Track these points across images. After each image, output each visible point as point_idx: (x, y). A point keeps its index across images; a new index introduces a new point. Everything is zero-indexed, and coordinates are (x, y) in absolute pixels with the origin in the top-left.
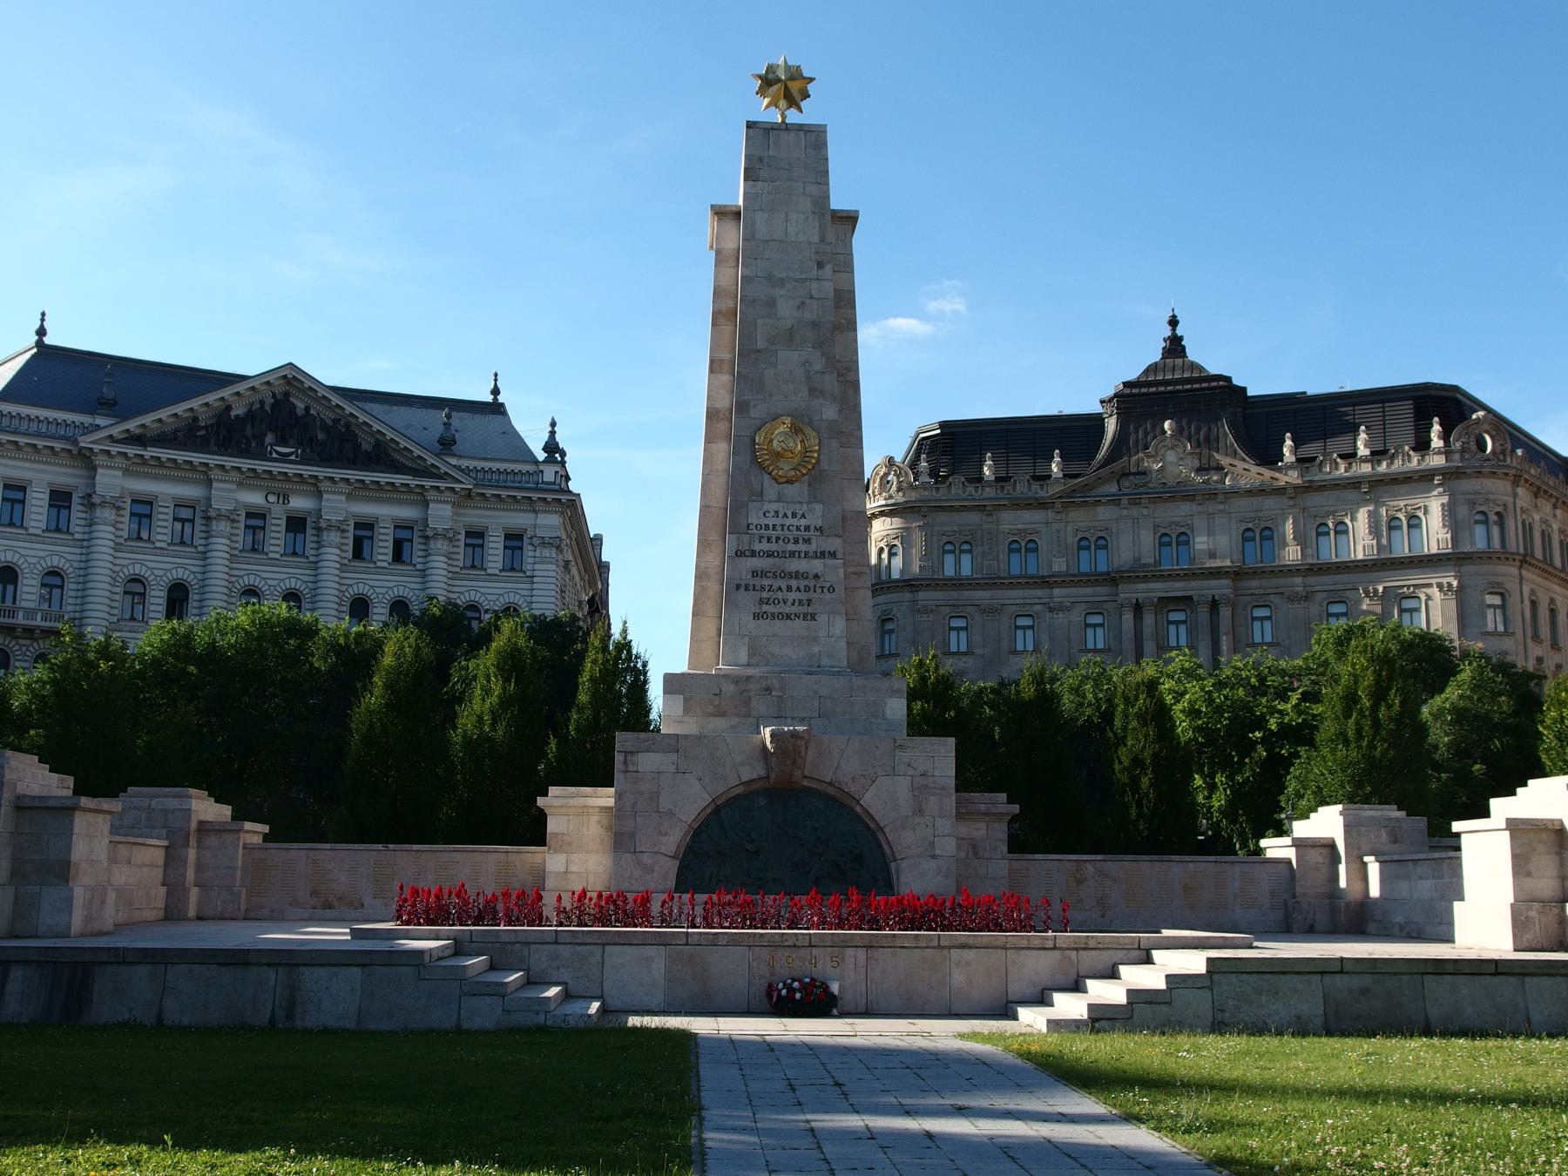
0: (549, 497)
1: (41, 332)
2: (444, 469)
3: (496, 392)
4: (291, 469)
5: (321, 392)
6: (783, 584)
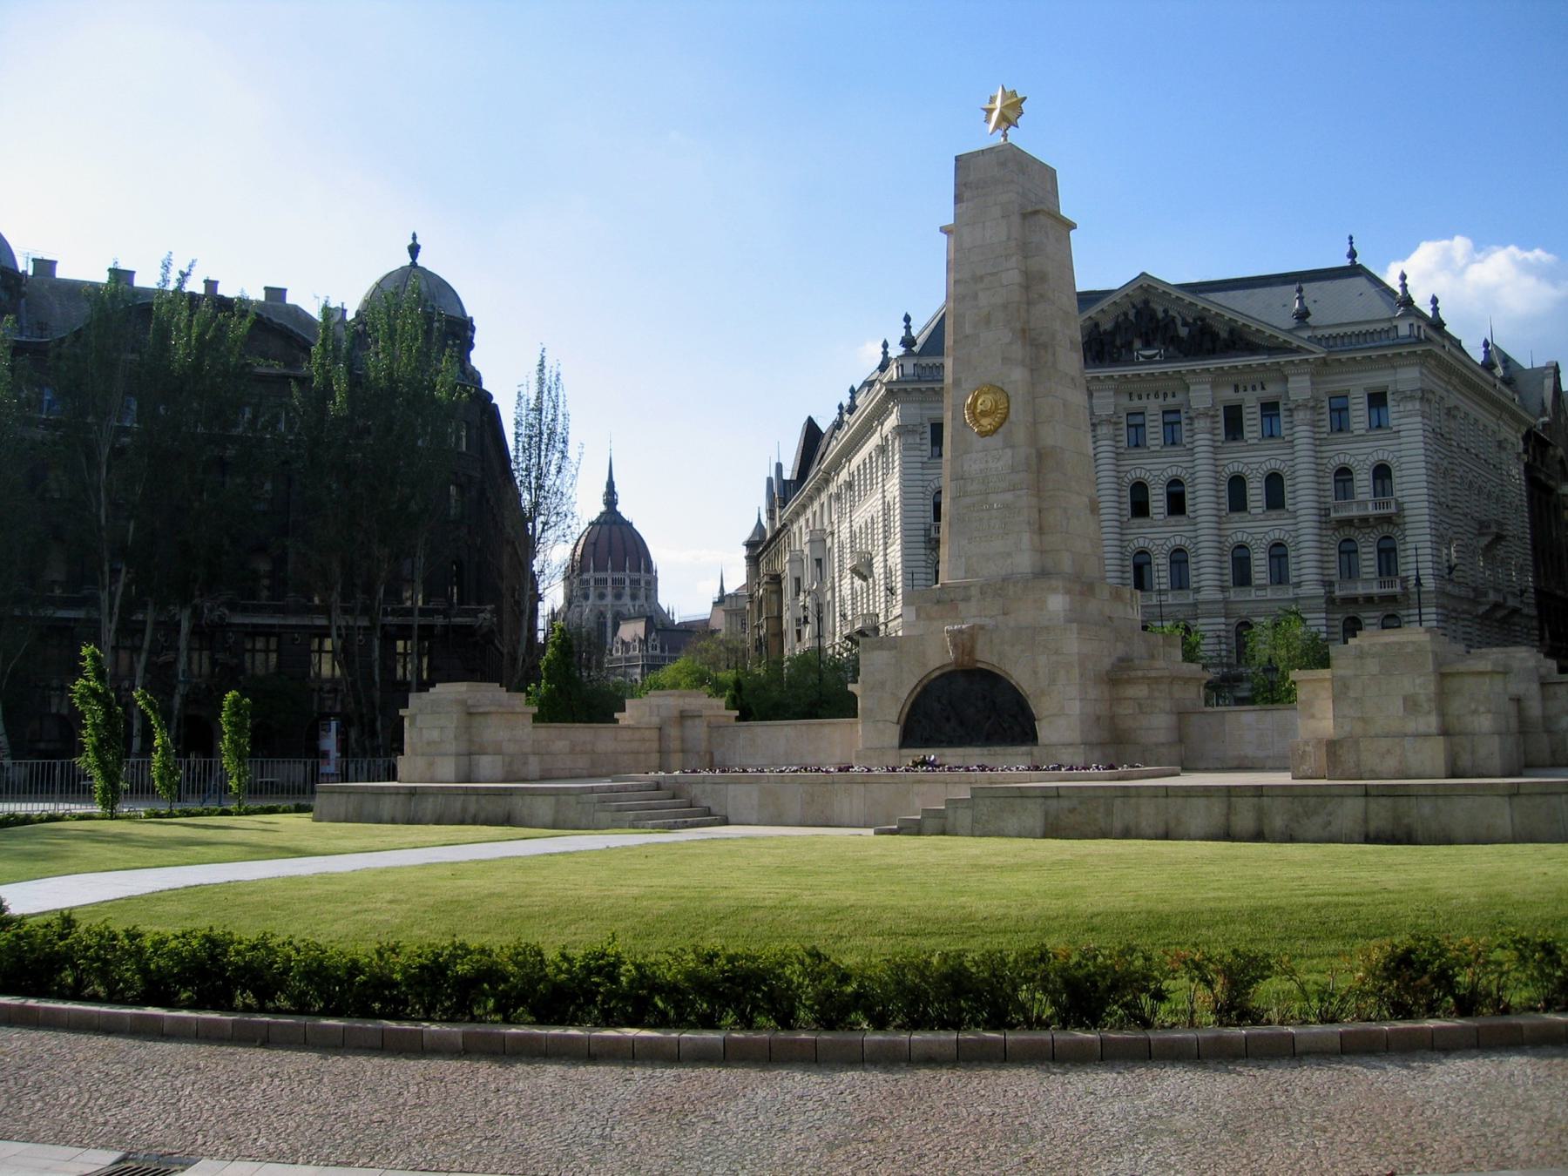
0: (1404, 351)
2: (1295, 343)
3: (1352, 254)
4: (1156, 369)
5: (1175, 294)
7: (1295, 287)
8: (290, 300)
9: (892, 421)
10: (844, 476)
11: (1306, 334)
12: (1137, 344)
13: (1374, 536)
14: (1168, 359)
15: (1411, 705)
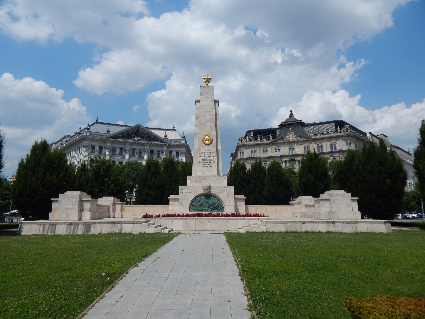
1: (97, 120)
3: (174, 128)
6: (206, 161)
12: (136, 137)
14: (141, 140)
15: (347, 205)
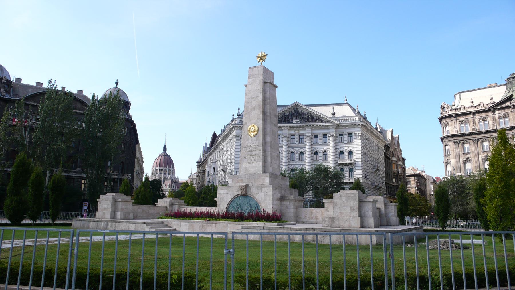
2: (332, 120)
4: (298, 125)
5: (304, 107)
7: (332, 107)
8: (84, 94)
9: (234, 134)
10: (221, 146)
11: (334, 119)
12: (294, 118)
13: (348, 168)
14: (301, 122)
15: (352, 209)
